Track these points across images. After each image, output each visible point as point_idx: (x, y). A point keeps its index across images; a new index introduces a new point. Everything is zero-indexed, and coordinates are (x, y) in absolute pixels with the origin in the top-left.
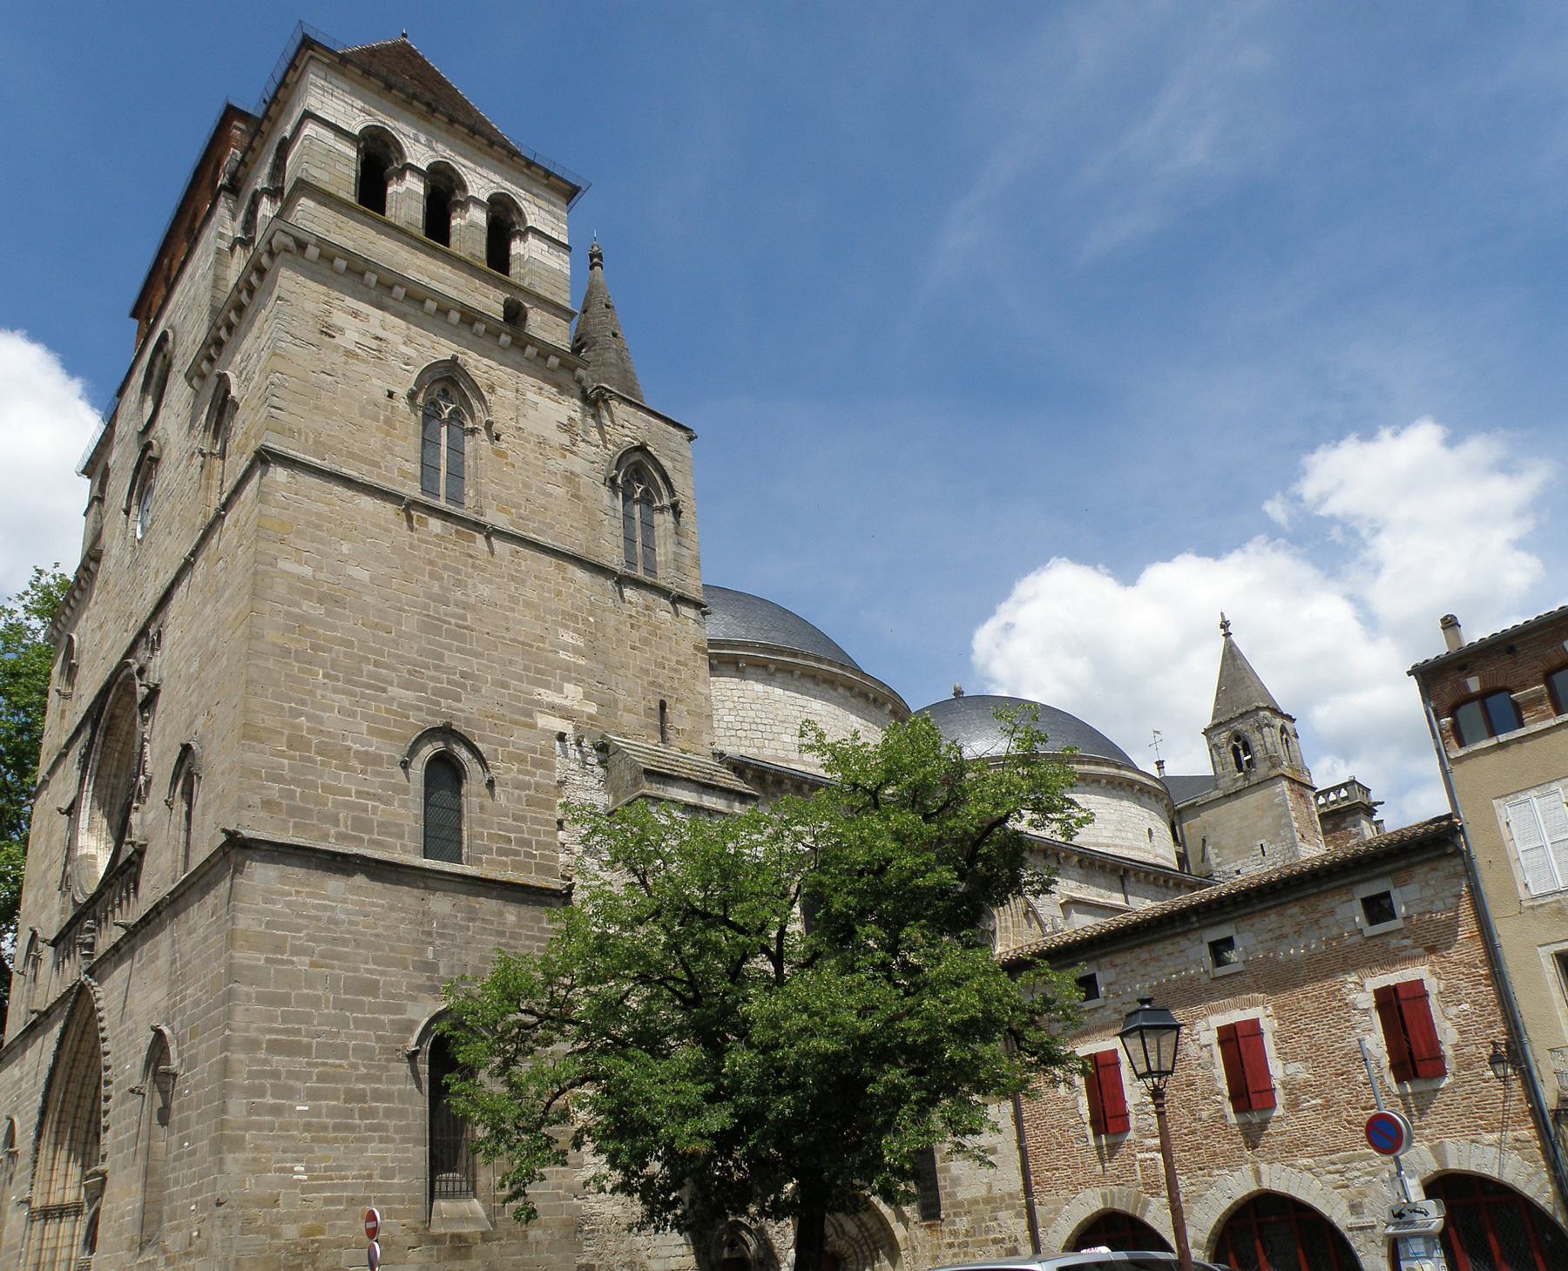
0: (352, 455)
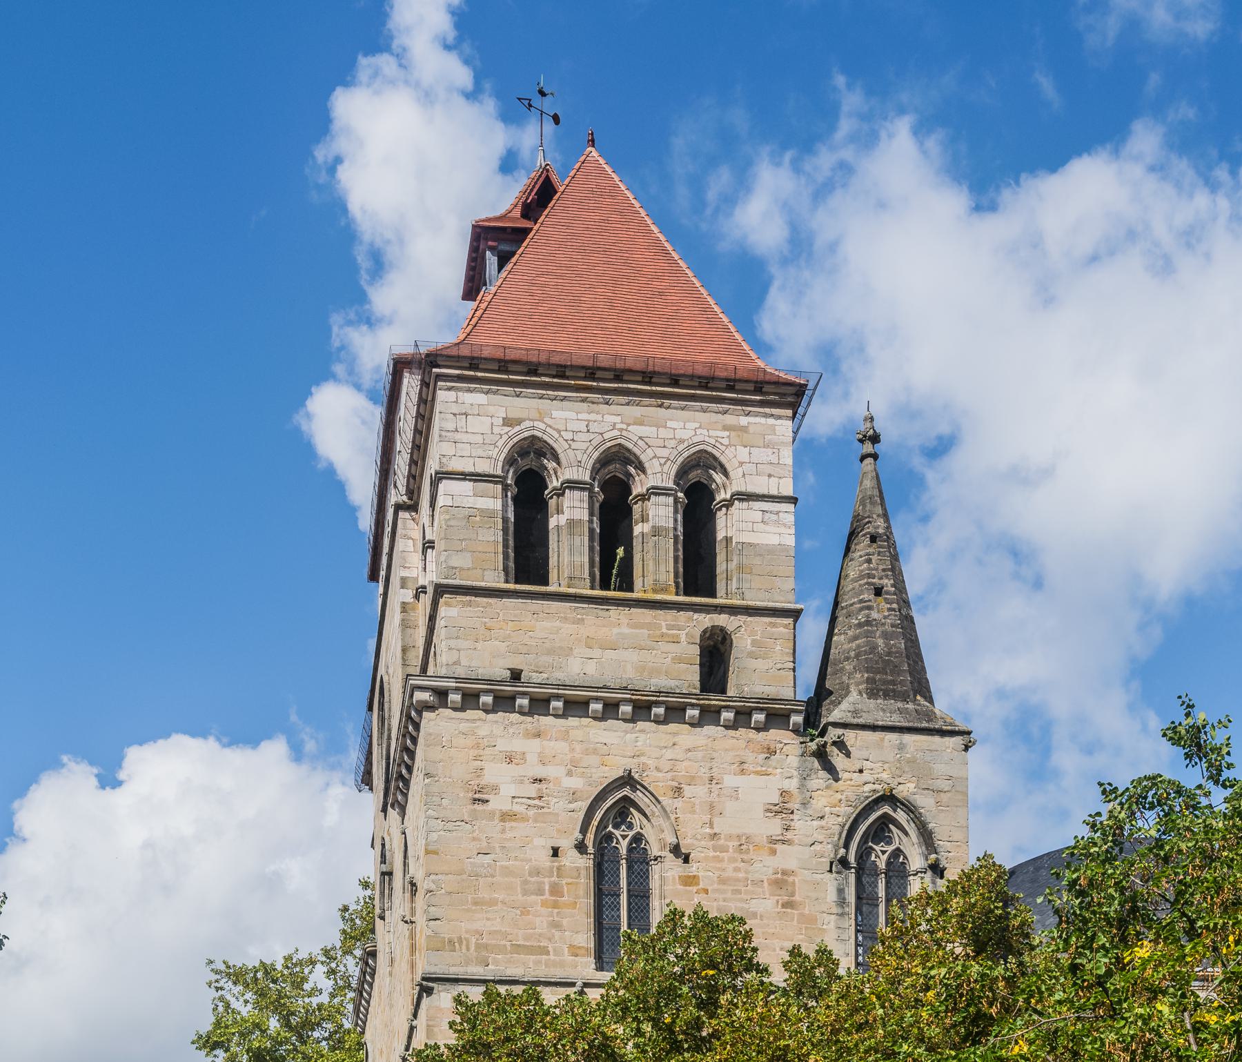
0: (518, 949)
